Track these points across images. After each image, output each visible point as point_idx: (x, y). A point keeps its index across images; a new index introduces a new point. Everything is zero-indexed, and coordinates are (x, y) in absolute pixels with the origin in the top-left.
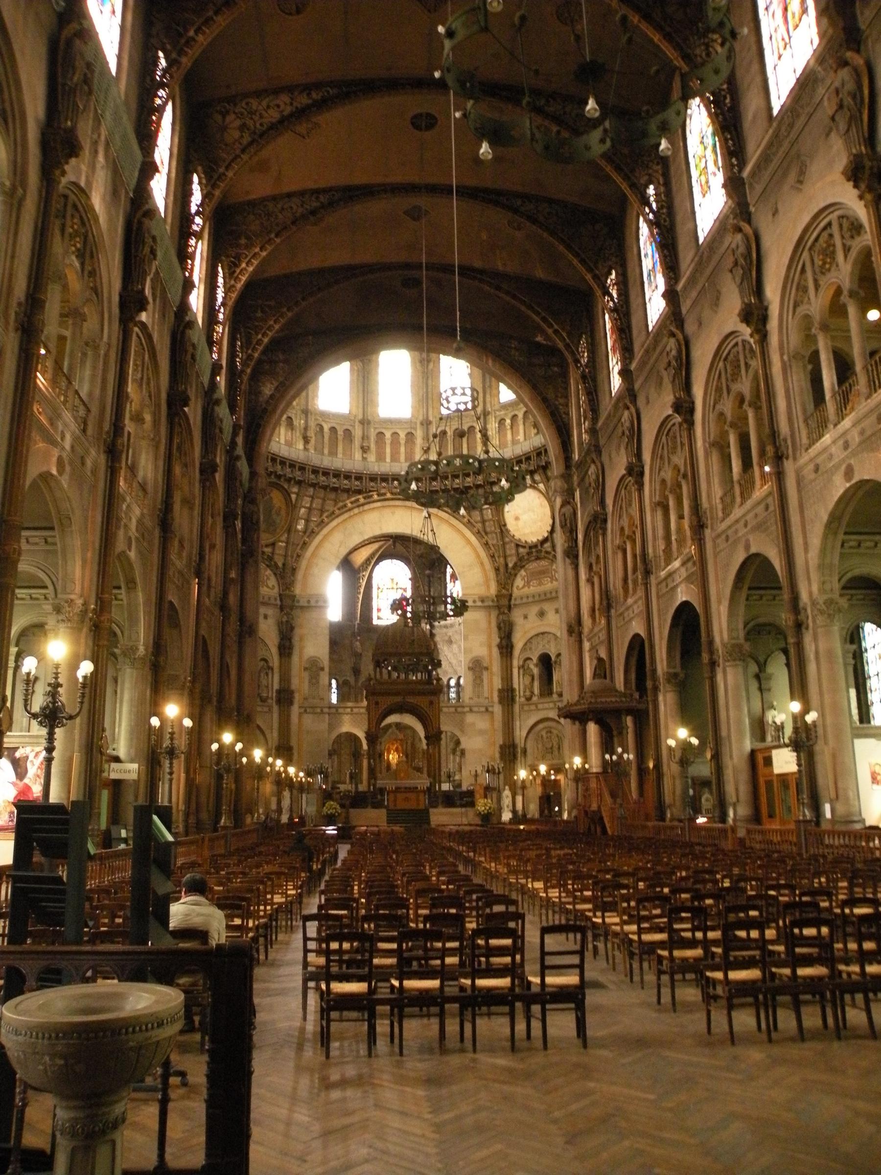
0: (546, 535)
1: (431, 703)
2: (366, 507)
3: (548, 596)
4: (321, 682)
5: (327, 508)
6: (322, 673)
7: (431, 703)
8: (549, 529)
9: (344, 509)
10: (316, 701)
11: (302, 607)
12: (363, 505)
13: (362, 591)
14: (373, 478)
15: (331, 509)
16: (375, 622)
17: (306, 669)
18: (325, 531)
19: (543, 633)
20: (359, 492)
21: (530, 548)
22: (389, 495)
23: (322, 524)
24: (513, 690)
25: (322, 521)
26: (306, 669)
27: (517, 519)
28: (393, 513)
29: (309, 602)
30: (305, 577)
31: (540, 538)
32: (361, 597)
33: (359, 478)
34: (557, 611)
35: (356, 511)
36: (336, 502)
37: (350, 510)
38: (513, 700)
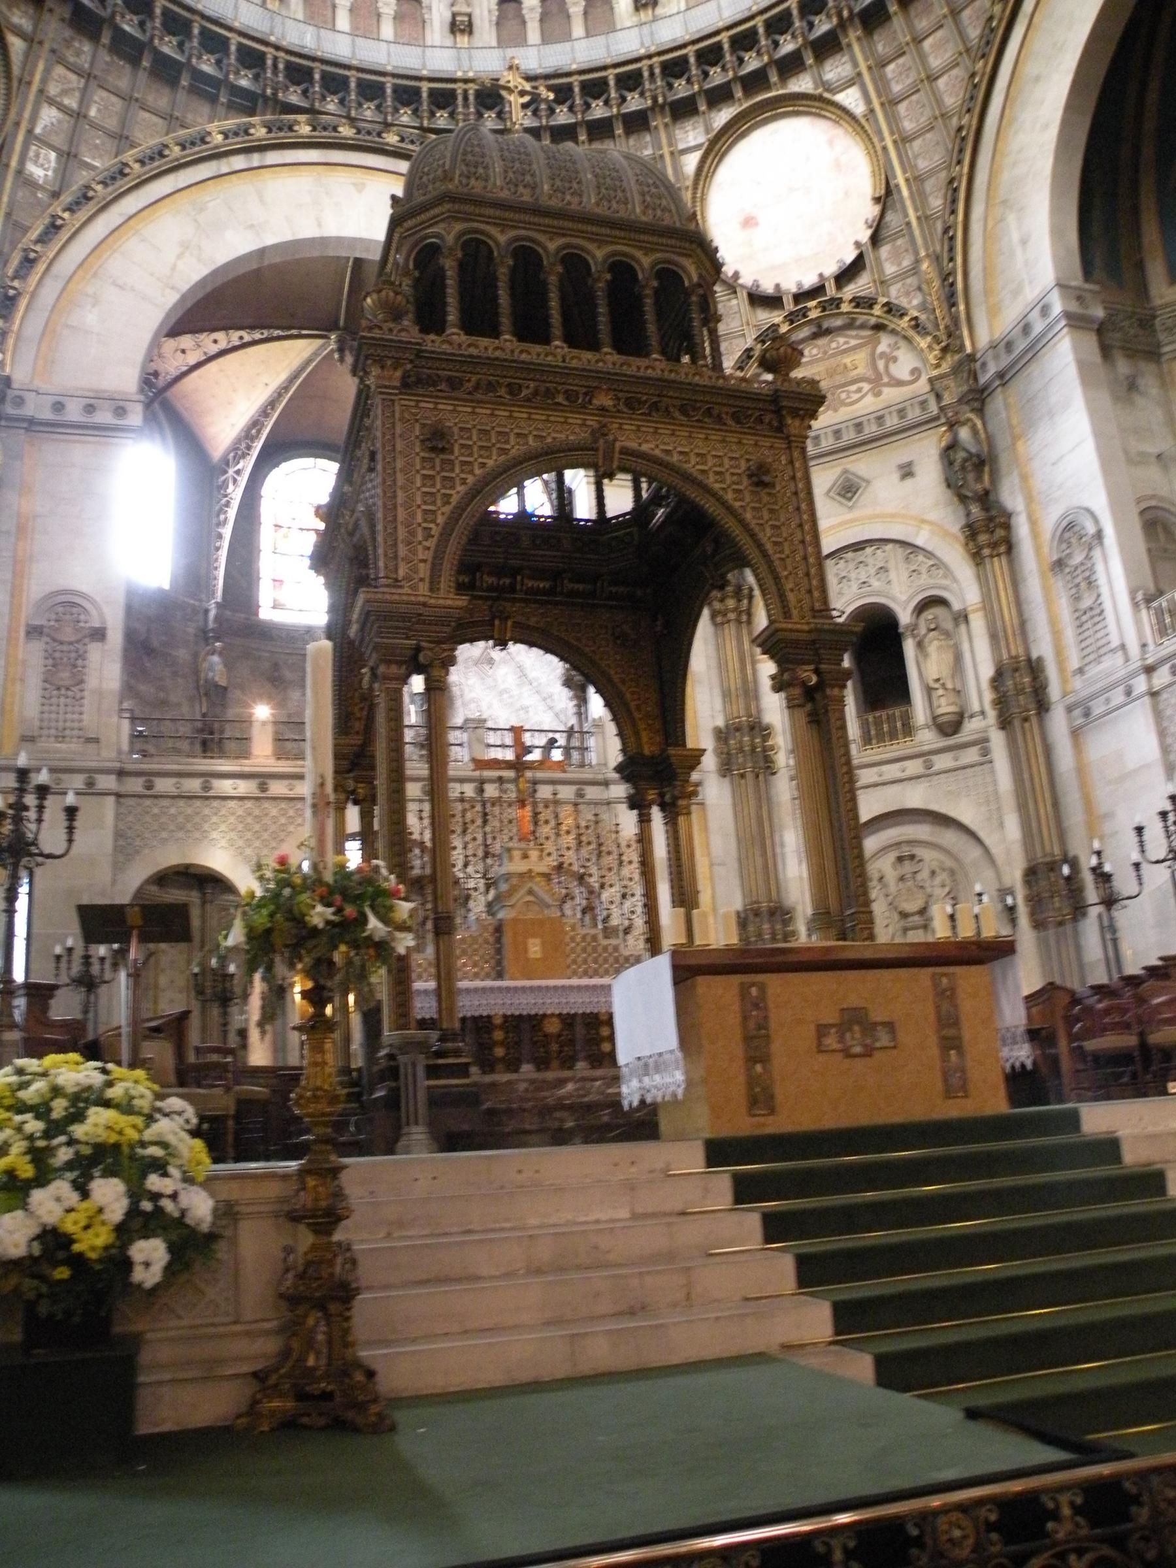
0: (850, 256)
1: (760, 478)
2: (273, 157)
3: (871, 429)
4: (92, 682)
5: (138, 135)
6: (95, 652)
7: (760, 478)
8: (865, 235)
9: (199, 151)
10: (70, 749)
11: (32, 425)
12: (262, 149)
13: (232, 513)
14: (300, 69)
15: (156, 141)
16: (266, 613)
17: (34, 632)
18: (131, 203)
19: (858, 547)
20: (248, 103)
21: (801, 297)
22: (346, 131)
23: (122, 182)
24: (759, 729)
25: (122, 172)
26: (34, 632)
27: (749, 222)
28: (360, 188)
29: (59, 407)
30: (48, 330)
31: (831, 269)
32: (227, 532)
33: (252, 58)
34: (907, 472)
35: (238, 162)
36: (172, 120)
37: (218, 155)
38: (766, 766)
